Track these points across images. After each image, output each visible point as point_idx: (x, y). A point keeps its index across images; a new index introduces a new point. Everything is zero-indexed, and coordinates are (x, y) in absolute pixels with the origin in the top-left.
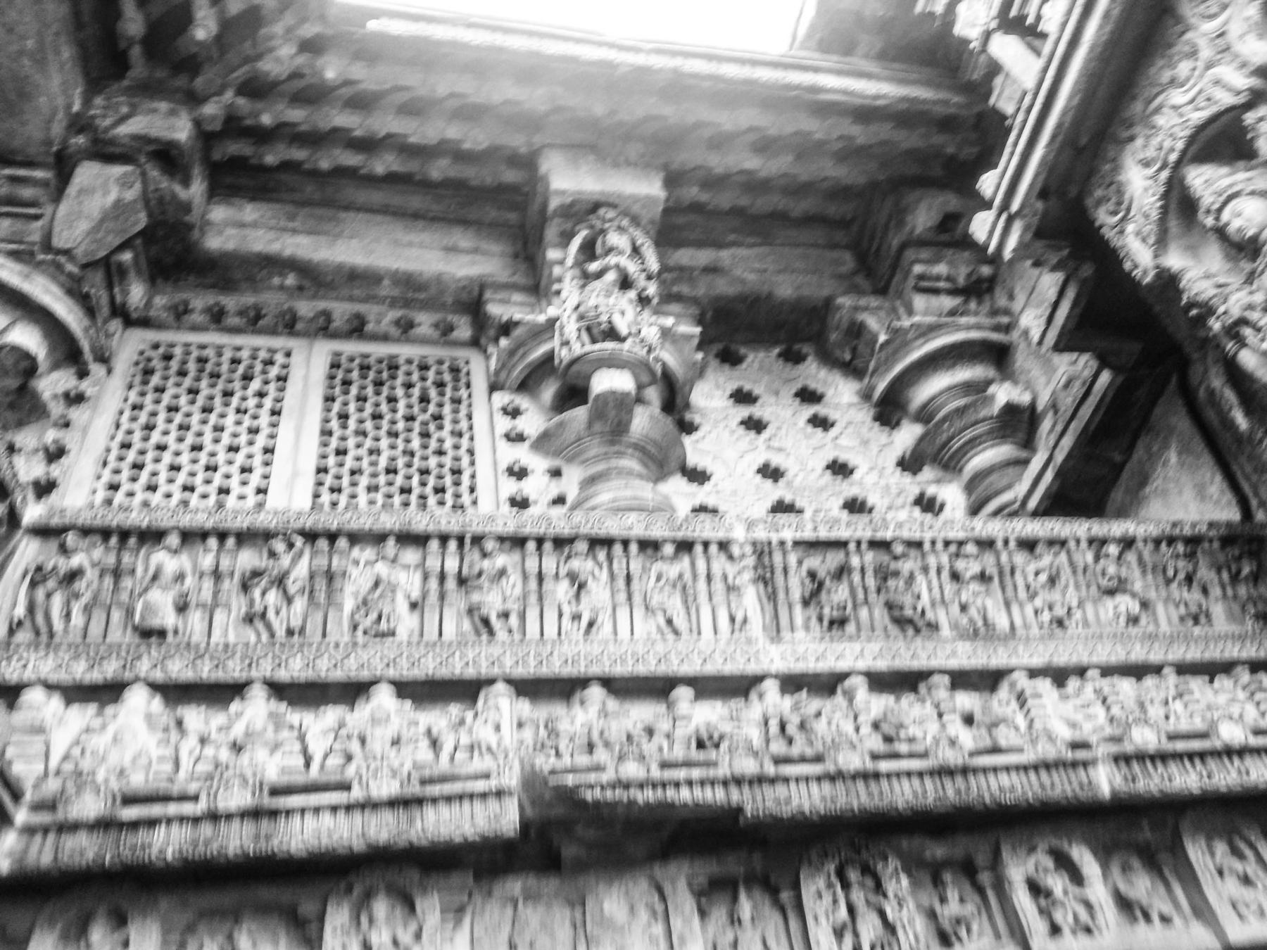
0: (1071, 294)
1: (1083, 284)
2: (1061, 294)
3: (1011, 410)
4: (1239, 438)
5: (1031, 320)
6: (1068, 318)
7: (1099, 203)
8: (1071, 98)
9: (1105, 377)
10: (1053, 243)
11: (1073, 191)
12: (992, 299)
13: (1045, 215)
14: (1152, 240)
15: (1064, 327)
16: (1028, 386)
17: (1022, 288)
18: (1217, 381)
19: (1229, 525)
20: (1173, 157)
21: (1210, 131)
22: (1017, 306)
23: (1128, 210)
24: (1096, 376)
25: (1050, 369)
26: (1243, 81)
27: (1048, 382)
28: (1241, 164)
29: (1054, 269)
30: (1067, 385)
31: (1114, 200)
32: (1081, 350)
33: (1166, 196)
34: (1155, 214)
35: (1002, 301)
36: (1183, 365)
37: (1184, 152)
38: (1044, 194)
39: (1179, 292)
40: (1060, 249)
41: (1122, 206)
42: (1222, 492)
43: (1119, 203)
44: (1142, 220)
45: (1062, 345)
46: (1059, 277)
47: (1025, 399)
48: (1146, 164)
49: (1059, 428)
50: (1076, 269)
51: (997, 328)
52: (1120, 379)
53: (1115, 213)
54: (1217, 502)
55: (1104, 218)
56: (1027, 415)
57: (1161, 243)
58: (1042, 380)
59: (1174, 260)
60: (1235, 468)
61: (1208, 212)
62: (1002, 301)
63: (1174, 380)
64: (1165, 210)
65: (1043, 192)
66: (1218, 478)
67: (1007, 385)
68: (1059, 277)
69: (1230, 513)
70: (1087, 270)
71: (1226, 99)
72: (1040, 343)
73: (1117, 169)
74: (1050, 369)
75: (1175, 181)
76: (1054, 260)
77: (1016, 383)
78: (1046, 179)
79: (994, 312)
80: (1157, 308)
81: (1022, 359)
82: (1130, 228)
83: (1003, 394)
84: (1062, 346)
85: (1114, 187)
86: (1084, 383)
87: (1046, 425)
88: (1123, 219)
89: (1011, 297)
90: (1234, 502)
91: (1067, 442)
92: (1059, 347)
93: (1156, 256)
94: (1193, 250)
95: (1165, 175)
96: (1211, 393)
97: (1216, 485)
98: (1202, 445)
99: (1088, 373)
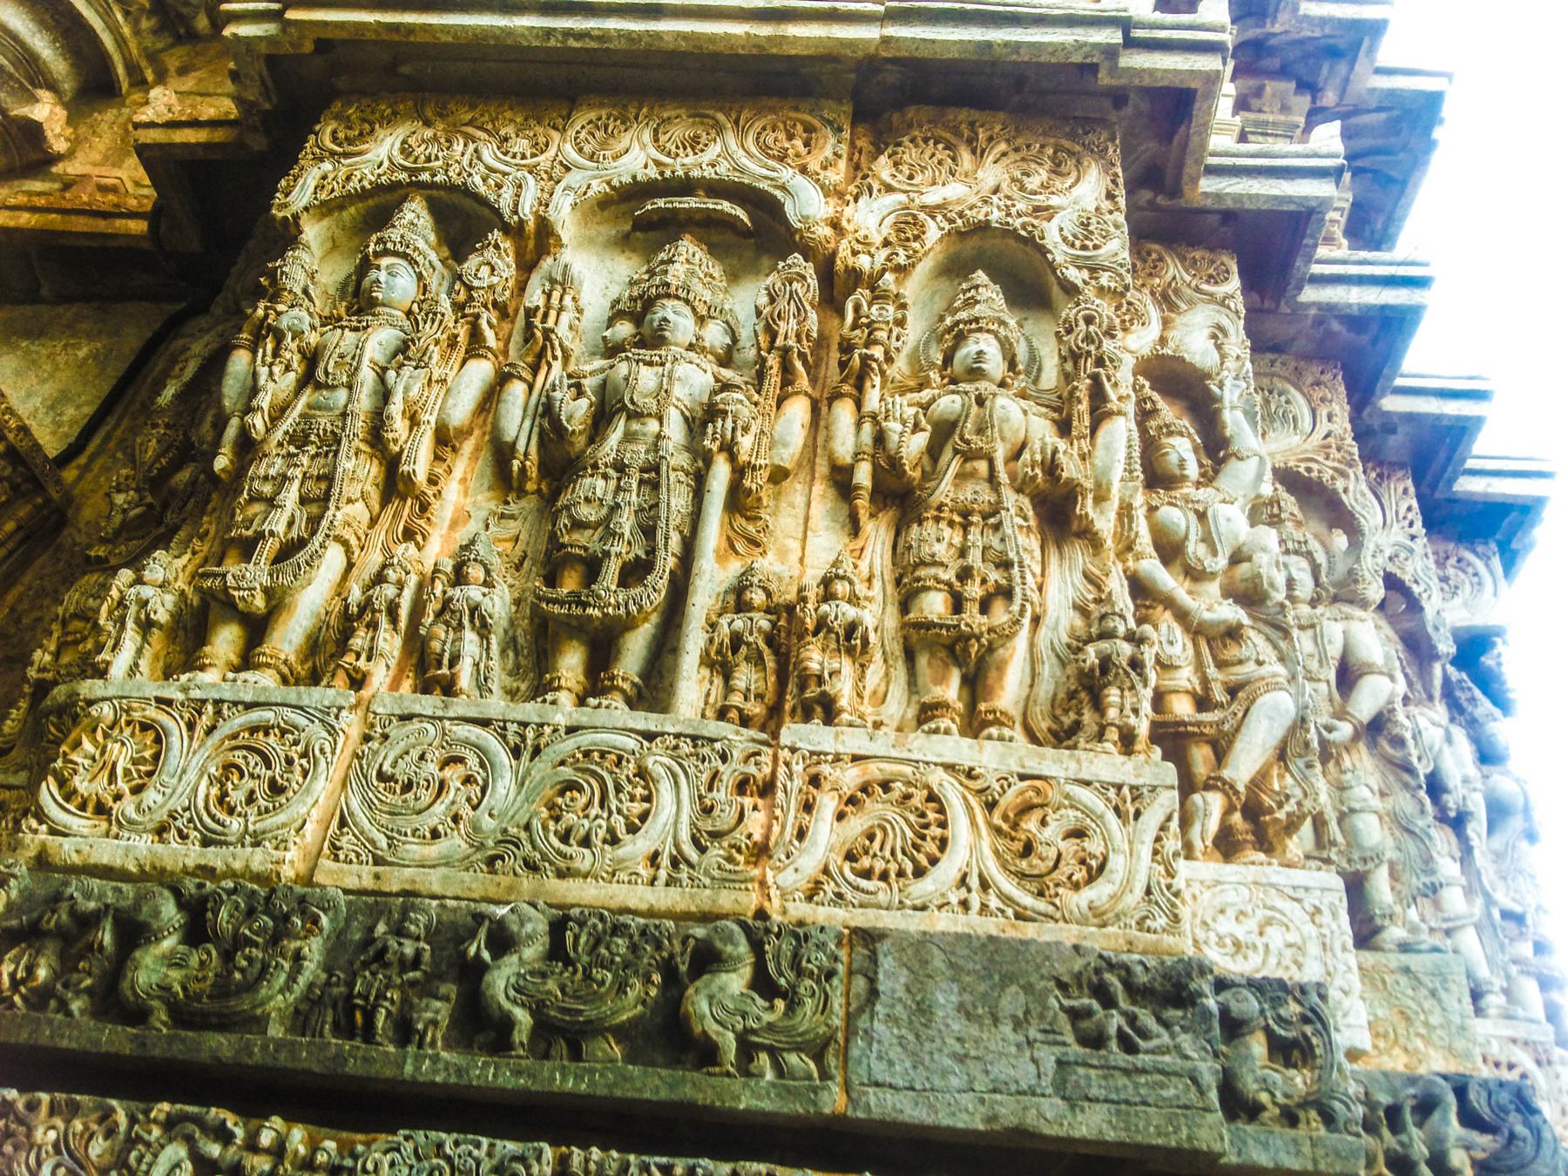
0: (219, 136)
1: (239, 144)
2: (213, 124)
3: (33, 132)
4: (148, 410)
5: (161, 102)
6: (186, 145)
7: (337, 117)
8: (445, 29)
9: (138, 227)
10: (270, 84)
11: (342, 83)
12: (172, 46)
13: (300, 58)
14: (323, 196)
15: (172, 145)
16: (76, 143)
17: (201, 80)
18: (199, 349)
19: (37, 447)
20: (425, 177)
21: (468, 203)
22: (176, 83)
23: (346, 155)
24: (132, 215)
25: (114, 158)
26: (527, 209)
27: (95, 164)
28: (446, 252)
29: (238, 100)
30: (104, 189)
31: (352, 134)
32: (156, 184)
33: (378, 188)
34: (354, 184)
35: (172, 62)
36: (199, 308)
37: (433, 186)
38: (323, 46)
39: (281, 255)
40: (269, 98)
41: (348, 147)
42: (72, 422)
43: (350, 141)
44: (342, 175)
45: (147, 154)
46: (234, 113)
47: (60, 146)
48: (406, 150)
49: (42, 202)
50: (254, 129)
51: (132, 69)
52: (144, 245)
53: (335, 139)
54: (59, 425)
55: (326, 132)
56: (35, 156)
57: (325, 209)
58: (97, 157)
59: (312, 232)
60: (111, 421)
61: (380, 241)
62: (172, 62)
63: (183, 305)
64: (363, 195)
65: (328, 43)
66: (88, 410)
67: (61, 113)
68: (234, 113)
69: (51, 446)
70: (258, 143)
71: (505, 202)
72: (137, 126)
73: (390, 121)
74: (114, 158)
75: (402, 192)
76: (251, 95)
77: (70, 121)
78: (344, 42)
79: (153, 57)
80: (251, 244)
81: (108, 120)
82: (327, 166)
83: (45, 111)
84: (151, 157)
85: (367, 127)
86: (117, 206)
87: (37, 186)
88: (333, 154)
89: (183, 71)
90: (72, 440)
91: (26, 219)
92: (142, 151)
93: (306, 209)
94: (334, 246)
95: (403, 176)
96: (186, 349)
97: (75, 414)
98: (120, 374)
99: (132, 203)
